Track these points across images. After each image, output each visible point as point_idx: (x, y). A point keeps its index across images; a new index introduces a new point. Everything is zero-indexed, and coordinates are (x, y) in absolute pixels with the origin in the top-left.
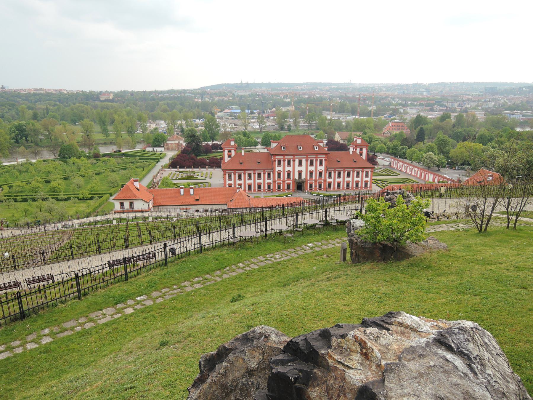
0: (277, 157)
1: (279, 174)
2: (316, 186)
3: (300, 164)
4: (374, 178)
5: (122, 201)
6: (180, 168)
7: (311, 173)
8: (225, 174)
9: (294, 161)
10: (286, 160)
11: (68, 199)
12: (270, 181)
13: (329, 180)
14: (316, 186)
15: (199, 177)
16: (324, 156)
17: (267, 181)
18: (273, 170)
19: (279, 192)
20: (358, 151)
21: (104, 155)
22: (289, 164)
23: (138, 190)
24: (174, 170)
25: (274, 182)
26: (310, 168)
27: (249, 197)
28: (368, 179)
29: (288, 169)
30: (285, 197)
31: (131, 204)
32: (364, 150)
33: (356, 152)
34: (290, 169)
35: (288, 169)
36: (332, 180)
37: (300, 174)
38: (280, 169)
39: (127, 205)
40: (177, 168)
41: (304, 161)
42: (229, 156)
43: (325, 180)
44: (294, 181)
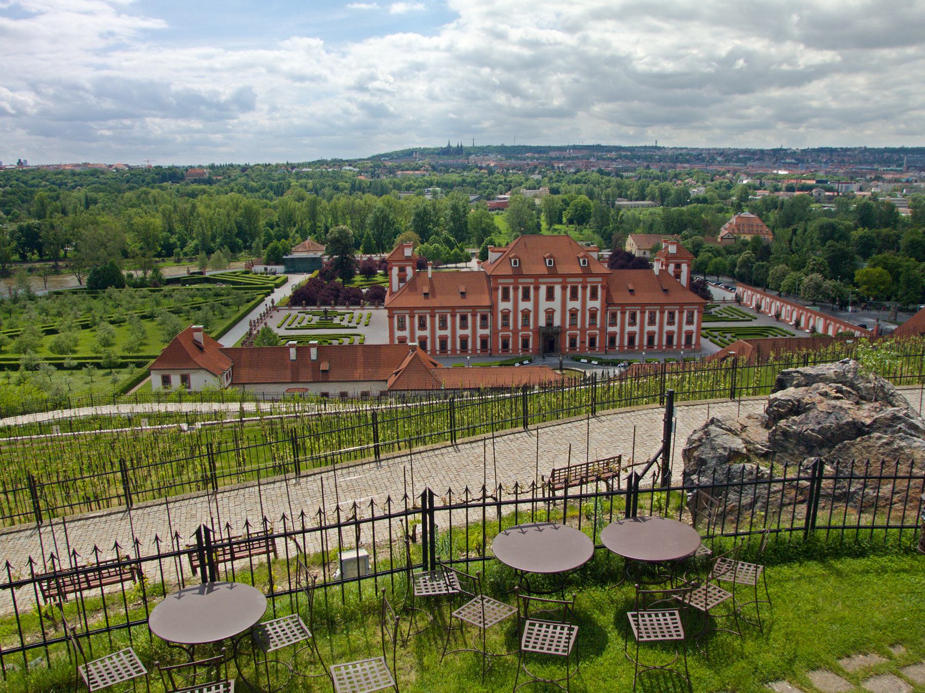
0: (500, 281)
1: (506, 316)
2: (583, 342)
3: (550, 296)
4: (704, 325)
5: (166, 373)
6: (308, 304)
7: (573, 314)
8: (391, 317)
9: (537, 289)
10: (521, 287)
11: (79, 367)
12: (487, 332)
13: (610, 329)
14: (583, 342)
15: (343, 323)
16: (600, 279)
17: (480, 332)
18: (493, 307)
19: (506, 354)
20: (671, 268)
21: (171, 281)
22: (526, 297)
23: (201, 349)
24: (295, 311)
25: (495, 332)
26: (571, 305)
27: (435, 365)
28: (693, 328)
29: (523, 305)
30: (517, 365)
31: (185, 379)
32: (684, 268)
33: (666, 270)
34: (529, 305)
35: (523, 305)
36: (616, 329)
37: (550, 314)
38: (509, 305)
39: (176, 380)
40: (301, 305)
41: (558, 290)
42: (402, 279)
43: (603, 330)
44: (538, 330)
